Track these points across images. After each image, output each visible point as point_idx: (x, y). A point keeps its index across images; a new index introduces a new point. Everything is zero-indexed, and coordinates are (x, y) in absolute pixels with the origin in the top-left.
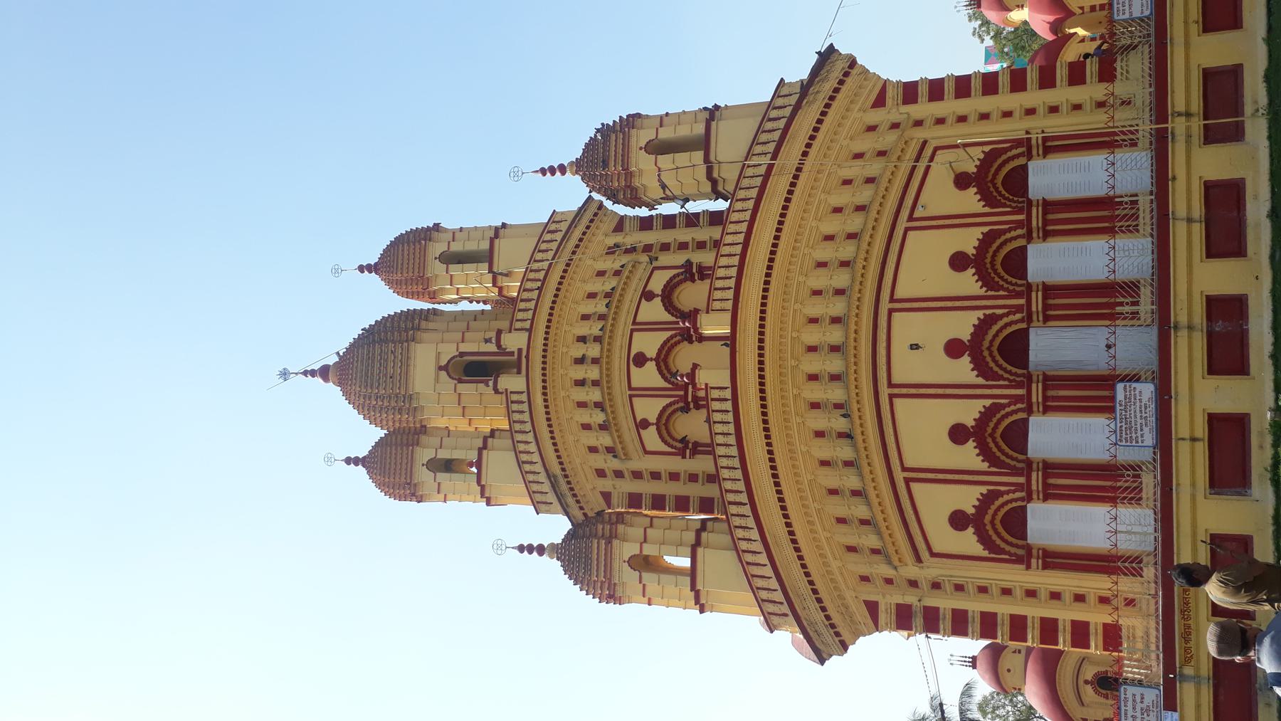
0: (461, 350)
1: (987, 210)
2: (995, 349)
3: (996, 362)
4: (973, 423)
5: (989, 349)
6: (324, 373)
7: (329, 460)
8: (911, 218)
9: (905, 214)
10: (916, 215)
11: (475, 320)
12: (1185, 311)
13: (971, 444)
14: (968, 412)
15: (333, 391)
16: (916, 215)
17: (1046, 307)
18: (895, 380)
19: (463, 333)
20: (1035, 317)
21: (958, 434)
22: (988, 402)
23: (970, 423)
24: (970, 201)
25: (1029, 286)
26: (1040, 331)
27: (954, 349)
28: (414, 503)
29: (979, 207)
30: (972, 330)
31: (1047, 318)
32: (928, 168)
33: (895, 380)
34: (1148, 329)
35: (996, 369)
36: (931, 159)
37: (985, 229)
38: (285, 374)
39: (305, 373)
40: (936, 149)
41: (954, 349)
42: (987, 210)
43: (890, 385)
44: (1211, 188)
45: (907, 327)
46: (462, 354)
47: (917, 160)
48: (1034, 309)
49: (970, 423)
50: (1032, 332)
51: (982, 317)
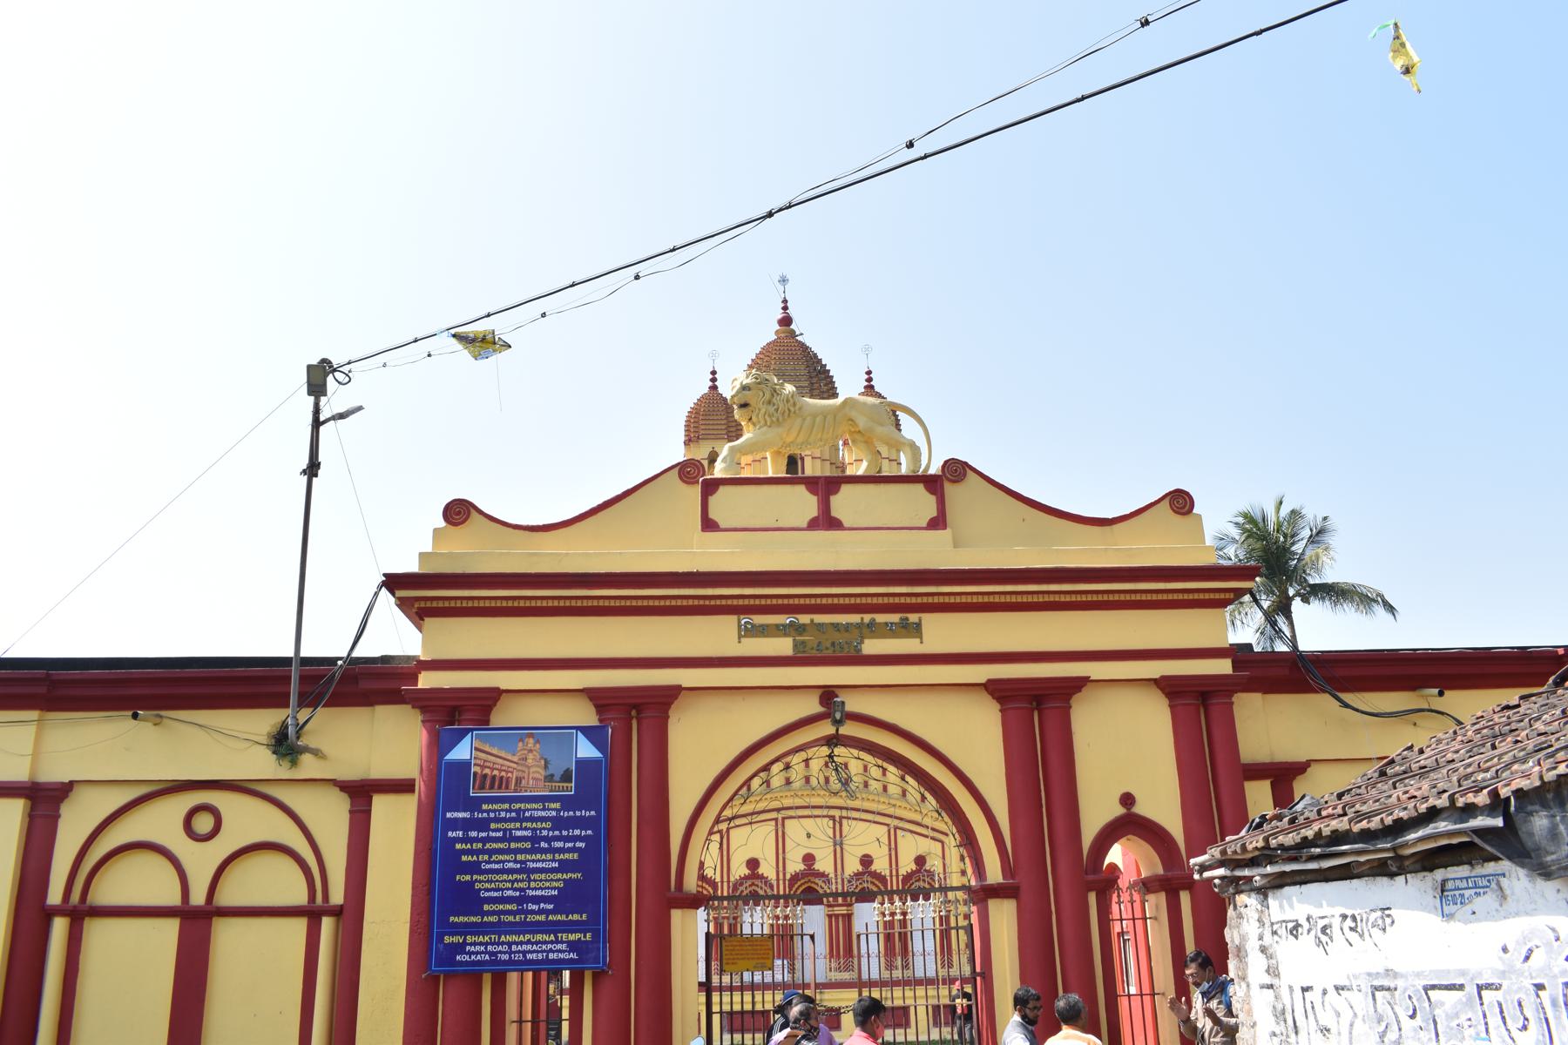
0: (805, 458)
1: (901, 878)
2: (809, 884)
3: (800, 887)
4: (760, 873)
5: (809, 881)
6: (786, 321)
7: (714, 355)
8: (896, 828)
9: (901, 824)
10: (899, 832)
11: (831, 464)
12: (830, 997)
13: (747, 872)
14: (767, 869)
15: (768, 332)
16: (899, 832)
17: (837, 916)
18: (787, 822)
19: (820, 458)
20: (830, 909)
21: (753, 864)
22: (775, 883)
23: (761, 871)
24: (907, 865)
25: (851, 905)
26: (822, 912)
27: (809, 859)
28: (682, 438)
29: (903, 872)
30: (821, 870)
31: (830, 916)
32: (926, 836)
33: (787, 822)
34: (824, 977)
35: (796, 886)
36: (933, 838)
37: (888, 878)
38: (784, 281)
39: (785, 301)
40: (942, 843)
41: (809, 859)
42: (901, 878)
43: (784, 819)
44: (905, 1010)
45: (821, 829)
46: (802, 459)
47: (933, 829)
48: (835, 909)
49: (761, 871)
50: (821, 907)
51: (830, 876)
